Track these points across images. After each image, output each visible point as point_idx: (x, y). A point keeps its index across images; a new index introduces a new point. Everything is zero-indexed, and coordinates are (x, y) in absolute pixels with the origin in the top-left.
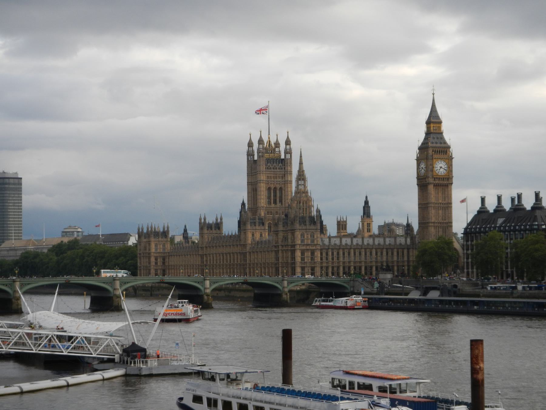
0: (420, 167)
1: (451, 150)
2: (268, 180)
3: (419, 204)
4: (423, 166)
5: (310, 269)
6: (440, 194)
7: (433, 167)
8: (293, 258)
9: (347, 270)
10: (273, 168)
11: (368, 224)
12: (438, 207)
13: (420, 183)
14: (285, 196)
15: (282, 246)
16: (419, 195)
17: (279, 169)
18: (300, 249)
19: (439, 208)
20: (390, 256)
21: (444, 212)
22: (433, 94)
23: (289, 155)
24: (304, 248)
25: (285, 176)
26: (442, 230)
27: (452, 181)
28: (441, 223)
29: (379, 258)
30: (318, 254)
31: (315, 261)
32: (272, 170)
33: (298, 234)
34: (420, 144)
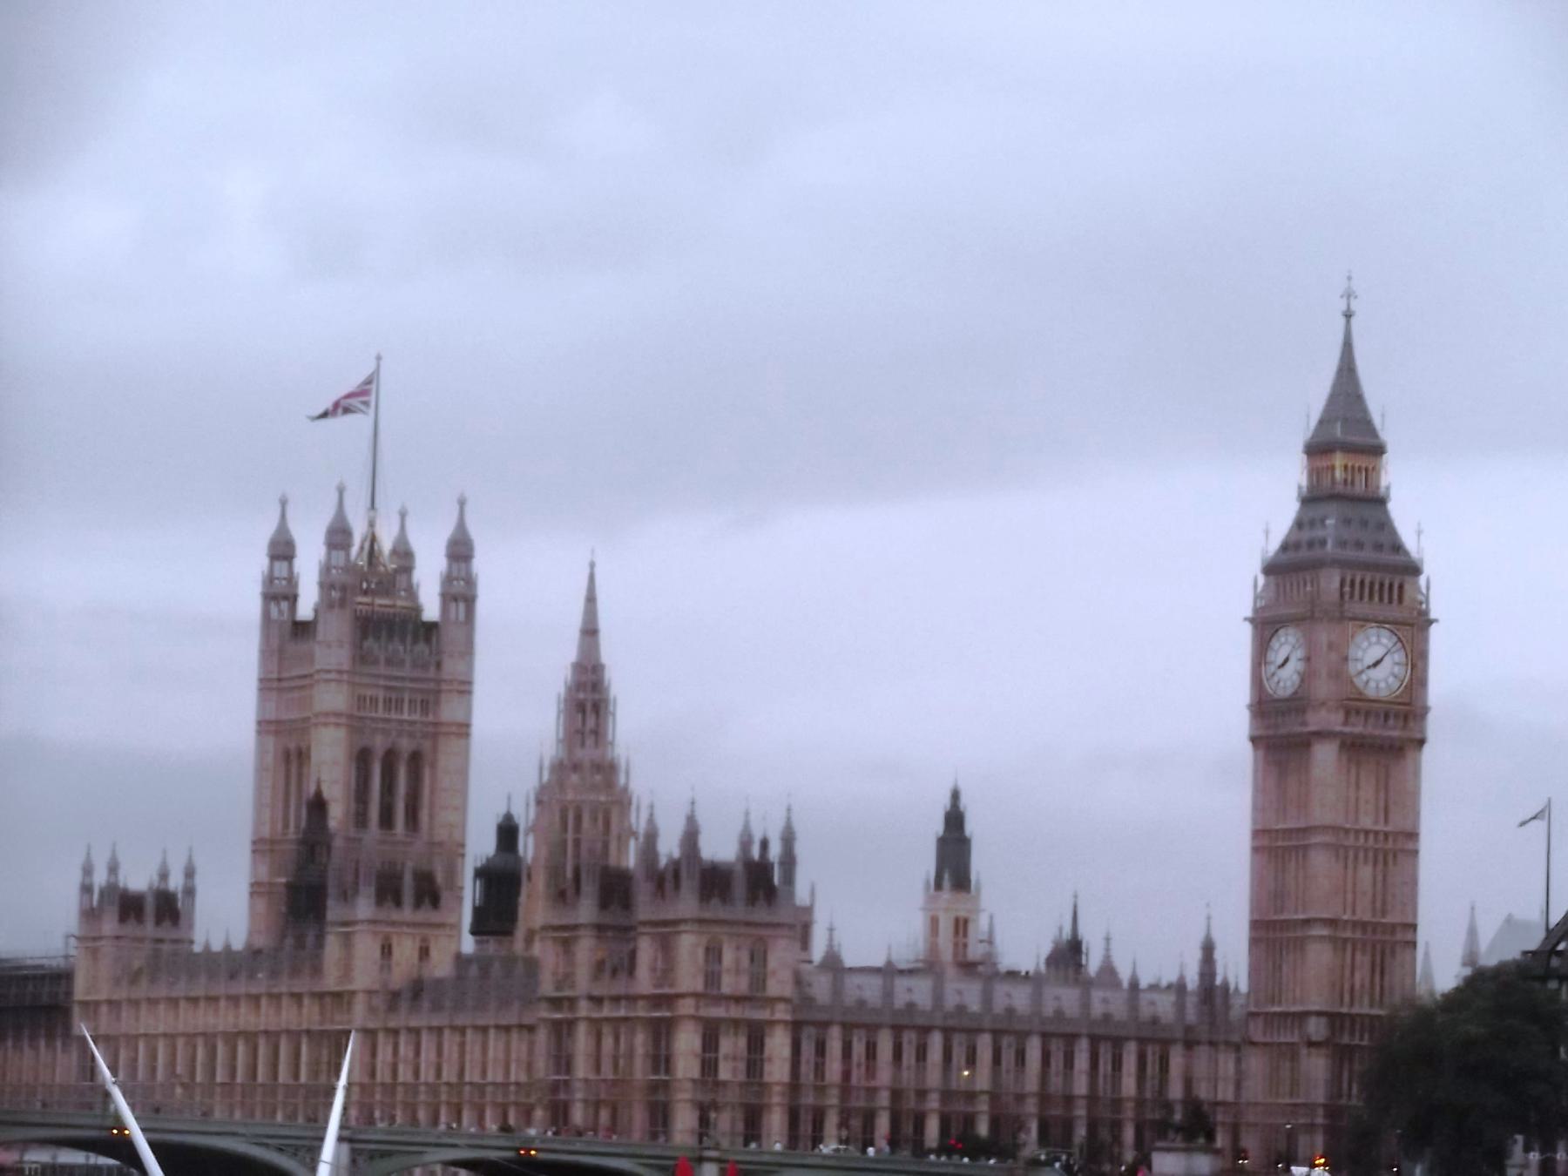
0: (1271, 656)
1: (1422, 580)
2: (362, 714)
3: (1257, 834)
4: (1287, 645)
5: (740, 1115)
6: (1368, 792)
7: (1346, 659)
8: (662, 1060)
9: (908, 1129)
10: (389, 662)
11: (957, 920)
12: (1357, 850)
13: (1271, 732)
14: (432, 792)
15: (597, 1001)
16: (1259, 790)
17: (415, 665)
19: (1361, 855)
20: (1105, 1076)
21: (1380, 878)
22: (1348, 315)
24: (718, 1012)
25: (437, 702)
26: (1367, 959)
27: (1422, 730)
28: (1363, 925)
29: (1056, 1083)
30: (778, 1045)
31: (767, 1079)
32: (382, 669)
33: (688, 945)
34: (1274, 545)
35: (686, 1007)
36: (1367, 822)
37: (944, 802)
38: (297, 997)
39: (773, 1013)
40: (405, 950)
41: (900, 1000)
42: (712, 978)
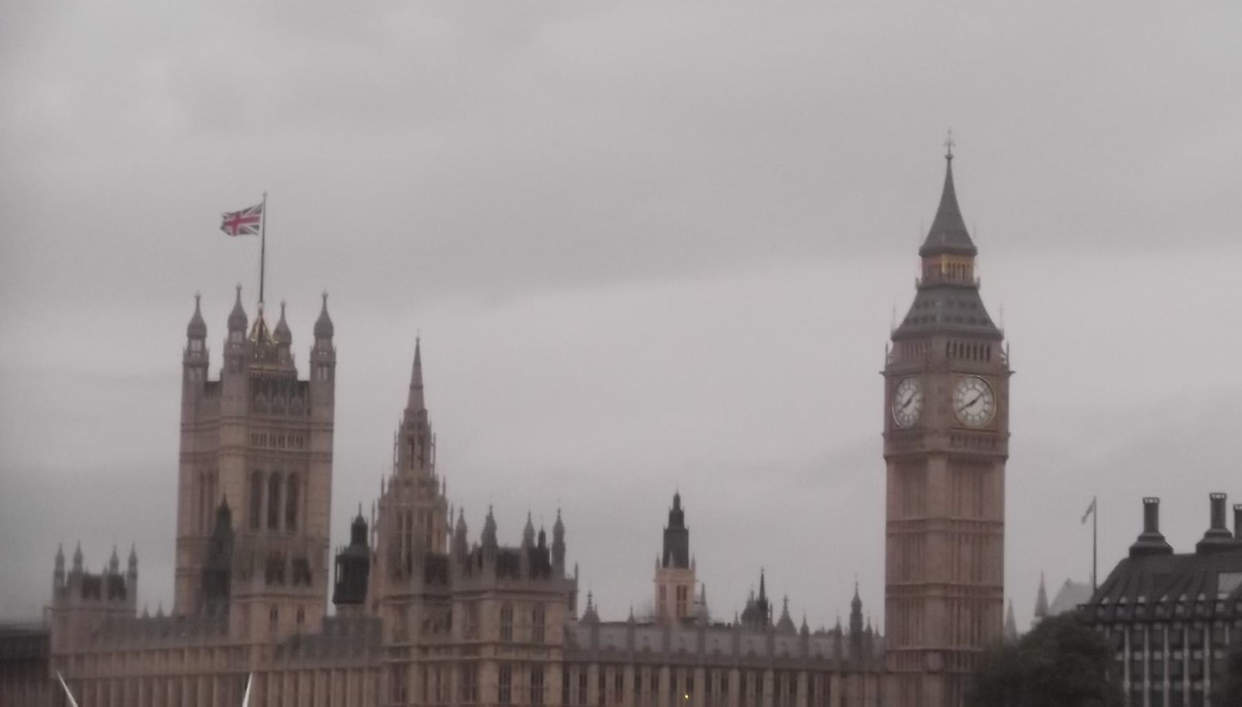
0: (899, 398)
1: (1004, 345)
3: (890, 524)
4: (908, 392)
7: (950, 400)
11: (678, 589)
14: (306, 501)
15: (424, 649)
18: (495, 660)
22: (949, 158)
23: (325, 370)
24: (511, 656)
27: (1006, 449)
30: (553, 679)
33: (489, 610)
34: (899, 321)
35: (487, 653)
36: (967, 515)
37: (670, 504)
38: (211, 651)
39: (549, 655)
40: (287, 615)
41: (639, 645)
42: (506, 631)
